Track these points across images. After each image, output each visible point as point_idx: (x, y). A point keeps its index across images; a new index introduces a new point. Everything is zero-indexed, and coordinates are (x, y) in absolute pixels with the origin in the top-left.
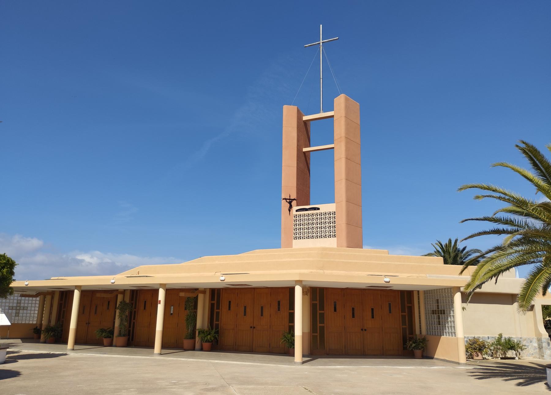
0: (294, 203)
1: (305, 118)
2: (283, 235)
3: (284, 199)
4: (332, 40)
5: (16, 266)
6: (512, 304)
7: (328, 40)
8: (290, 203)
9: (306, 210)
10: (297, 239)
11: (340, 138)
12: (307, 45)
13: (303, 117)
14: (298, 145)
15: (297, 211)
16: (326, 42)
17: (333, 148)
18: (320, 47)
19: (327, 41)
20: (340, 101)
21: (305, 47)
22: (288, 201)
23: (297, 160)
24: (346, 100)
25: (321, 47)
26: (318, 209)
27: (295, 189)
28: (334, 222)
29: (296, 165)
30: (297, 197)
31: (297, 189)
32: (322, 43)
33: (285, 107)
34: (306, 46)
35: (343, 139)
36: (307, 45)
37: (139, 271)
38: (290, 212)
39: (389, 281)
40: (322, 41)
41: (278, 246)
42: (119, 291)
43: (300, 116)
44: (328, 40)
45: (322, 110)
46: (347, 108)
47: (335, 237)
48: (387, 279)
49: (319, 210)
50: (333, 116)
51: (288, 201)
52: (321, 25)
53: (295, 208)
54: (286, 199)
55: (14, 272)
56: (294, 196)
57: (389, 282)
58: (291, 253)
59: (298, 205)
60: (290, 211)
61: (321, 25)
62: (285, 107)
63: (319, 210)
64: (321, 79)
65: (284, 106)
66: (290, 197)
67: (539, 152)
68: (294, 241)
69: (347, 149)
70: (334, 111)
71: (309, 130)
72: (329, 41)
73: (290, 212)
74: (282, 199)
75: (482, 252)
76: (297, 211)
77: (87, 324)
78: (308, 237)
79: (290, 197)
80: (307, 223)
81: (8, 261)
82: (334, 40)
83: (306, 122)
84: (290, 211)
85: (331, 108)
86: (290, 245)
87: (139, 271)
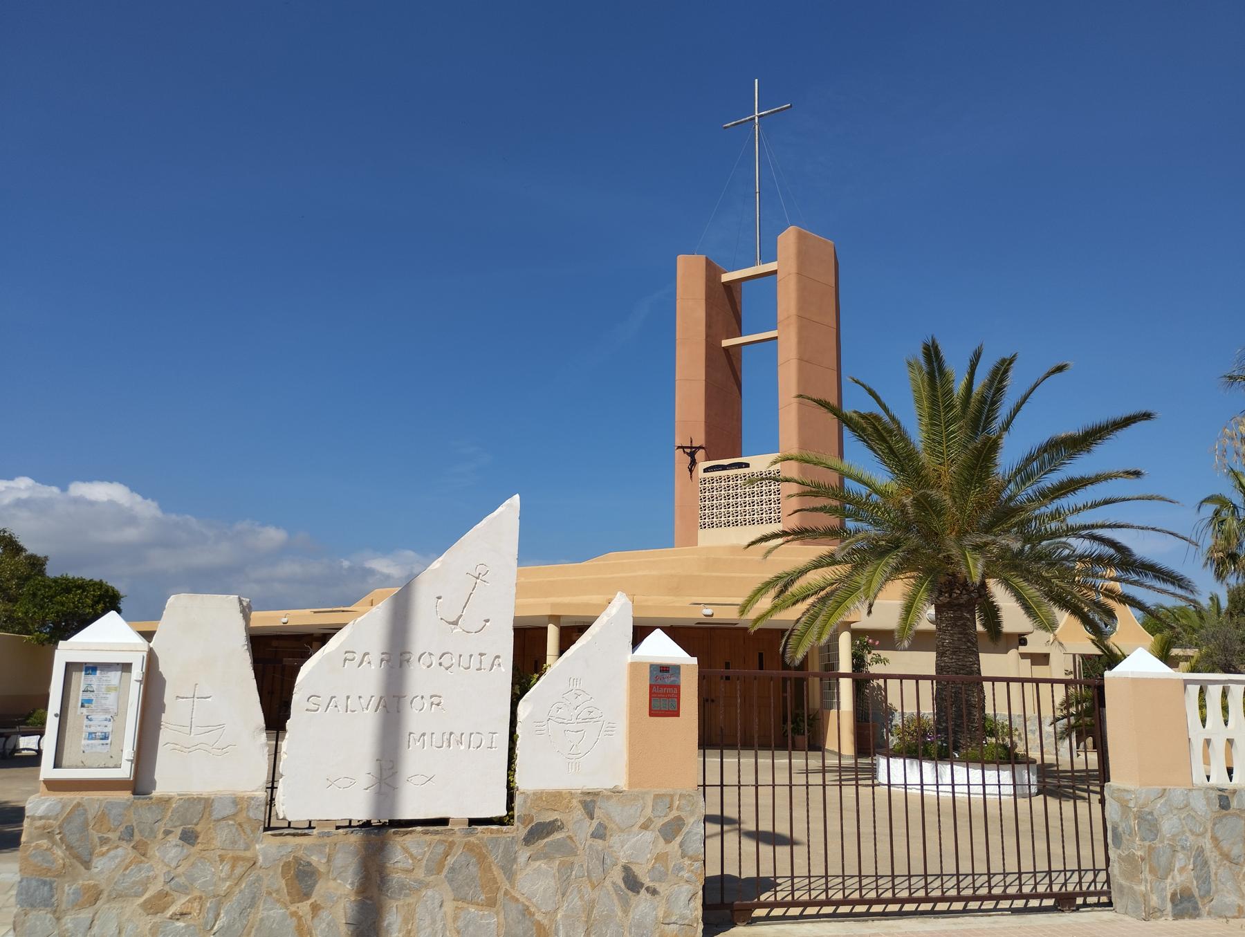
0: (700, 455)
1: (726, 278)
2: (677, 522)
3: (679, 447)
4: (778, 111)
5: (122, 599)
6: (1007, 653)
7: (769, 111)
8: (692, 455)
9: (724, 468)
10: (756, 523)
11: (788, 317)
12: (729, 124)
13: (722, 275)
14: (707, 336)
15: (706, 470)
16: (765, 115)
17: (776, 338)
18: (755, 128)
19: (769, 113)
20: (788, 240)
21: (726, 128)
22: (688, 451)
23: (707, 366)
24: (801, 238)
25: (757, 126)
26: (747, 465)
27: (702, 425)
28: (778, 491)
29: (704, 378)
30: (707, 441)
31: (705, 425)
32: (759, 117)
33: (681, 258)
34: (726, 125)
35: (794, 320)
36: (729, 124)
37: (372, 600)
38: (691, 474)
39: (710, 613)
40: (758, 113)
41: (669, 543)
42: (315, 635)
43: (712, 272)
44: (769, 111)
45: (758, 259)
46: (803, 256)
47: (779, 522)
48: (708, 612)
49: (749, 467)
50: (775, 272)
51: (688, 451)
52: (756, 80)
53: (702, 465)
54: (683, 448)
55: (121, 608)
56: (700, 440)
57: (712, 615)
58: (652, 559)
59: (708, 459)
60: (691, 471)
61: (756, 80)
62: (681, 258)
63: (749, 467)
64: (758, 194)
65: (678, 257)
66: (691, 442)
67: (36, 556)
68: (701, 532)
69: (802, 341)
70: (776, 260)
71: (737, 301)
72: (772, 112)
73: (691, 474)
74: (676, 448)
75: (1072, 546)
76: (706, 470)
77: (269, 692)
78: (728, 524)
79: (691, 442)
80: (759, 492)
81: (107, 591)
82: (781, 110)
83: (729, 286)
84: (691, 471)
85: (770, 255)
86: (693, 541)
87: (372, 600)
